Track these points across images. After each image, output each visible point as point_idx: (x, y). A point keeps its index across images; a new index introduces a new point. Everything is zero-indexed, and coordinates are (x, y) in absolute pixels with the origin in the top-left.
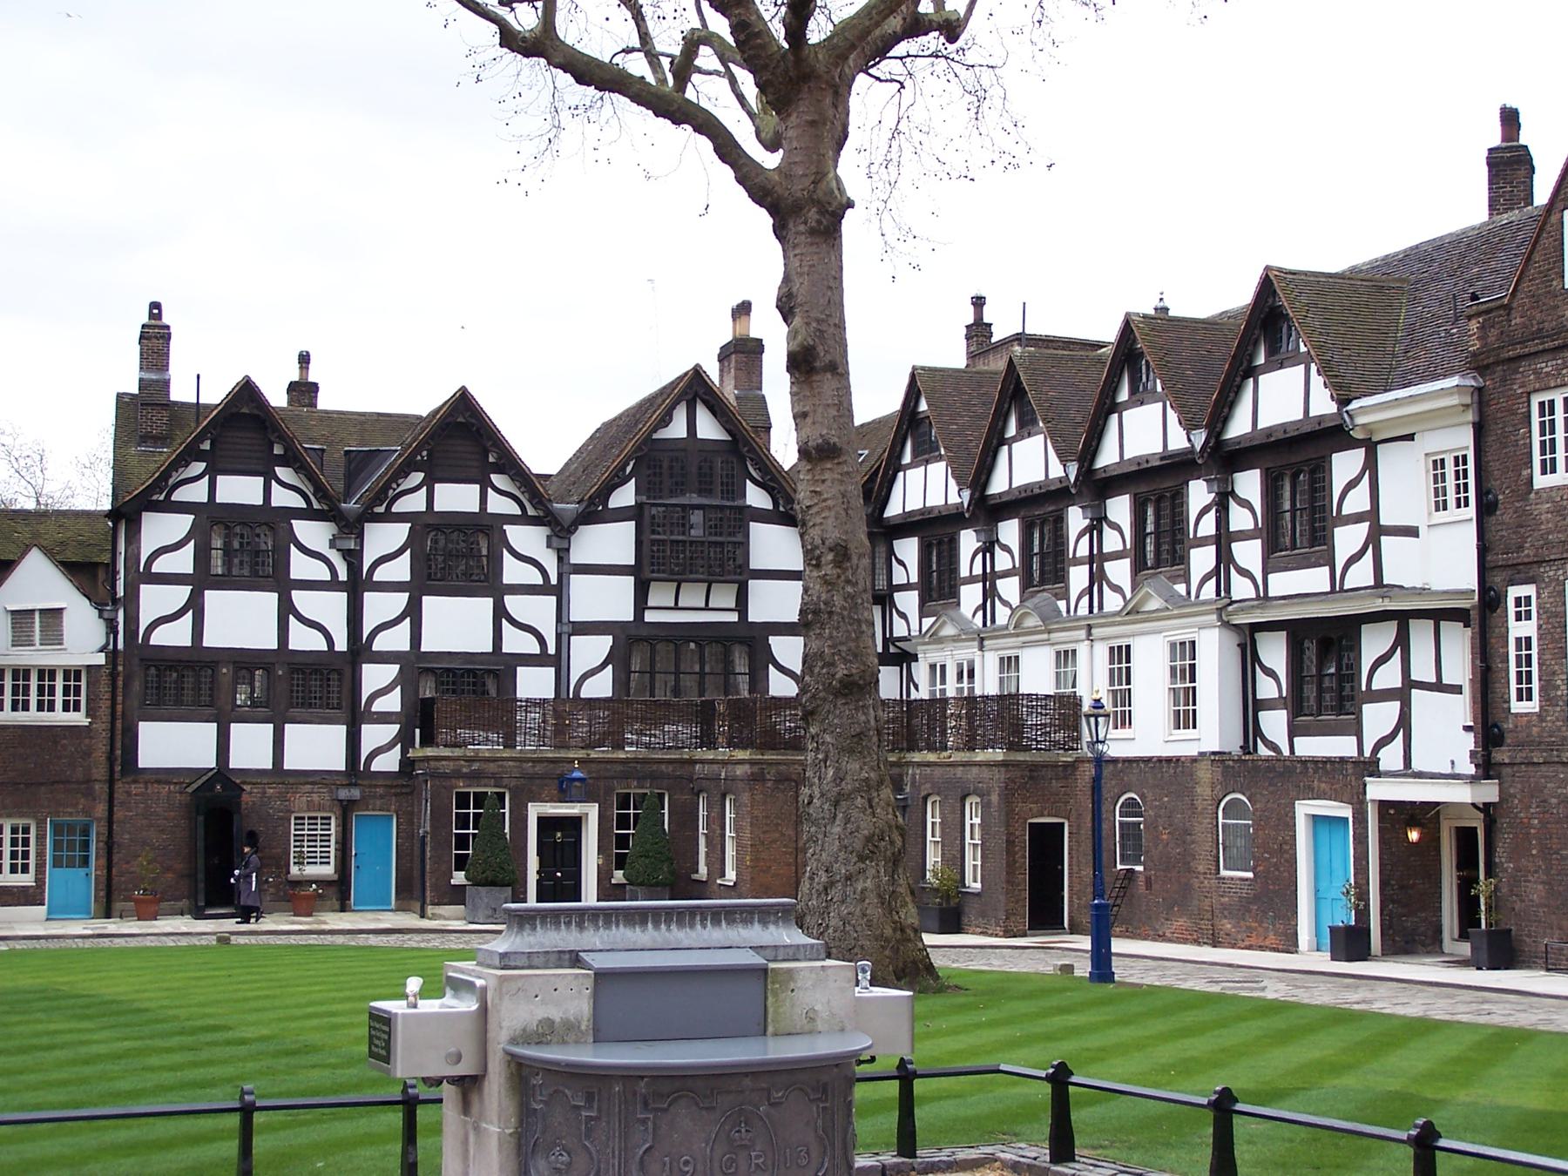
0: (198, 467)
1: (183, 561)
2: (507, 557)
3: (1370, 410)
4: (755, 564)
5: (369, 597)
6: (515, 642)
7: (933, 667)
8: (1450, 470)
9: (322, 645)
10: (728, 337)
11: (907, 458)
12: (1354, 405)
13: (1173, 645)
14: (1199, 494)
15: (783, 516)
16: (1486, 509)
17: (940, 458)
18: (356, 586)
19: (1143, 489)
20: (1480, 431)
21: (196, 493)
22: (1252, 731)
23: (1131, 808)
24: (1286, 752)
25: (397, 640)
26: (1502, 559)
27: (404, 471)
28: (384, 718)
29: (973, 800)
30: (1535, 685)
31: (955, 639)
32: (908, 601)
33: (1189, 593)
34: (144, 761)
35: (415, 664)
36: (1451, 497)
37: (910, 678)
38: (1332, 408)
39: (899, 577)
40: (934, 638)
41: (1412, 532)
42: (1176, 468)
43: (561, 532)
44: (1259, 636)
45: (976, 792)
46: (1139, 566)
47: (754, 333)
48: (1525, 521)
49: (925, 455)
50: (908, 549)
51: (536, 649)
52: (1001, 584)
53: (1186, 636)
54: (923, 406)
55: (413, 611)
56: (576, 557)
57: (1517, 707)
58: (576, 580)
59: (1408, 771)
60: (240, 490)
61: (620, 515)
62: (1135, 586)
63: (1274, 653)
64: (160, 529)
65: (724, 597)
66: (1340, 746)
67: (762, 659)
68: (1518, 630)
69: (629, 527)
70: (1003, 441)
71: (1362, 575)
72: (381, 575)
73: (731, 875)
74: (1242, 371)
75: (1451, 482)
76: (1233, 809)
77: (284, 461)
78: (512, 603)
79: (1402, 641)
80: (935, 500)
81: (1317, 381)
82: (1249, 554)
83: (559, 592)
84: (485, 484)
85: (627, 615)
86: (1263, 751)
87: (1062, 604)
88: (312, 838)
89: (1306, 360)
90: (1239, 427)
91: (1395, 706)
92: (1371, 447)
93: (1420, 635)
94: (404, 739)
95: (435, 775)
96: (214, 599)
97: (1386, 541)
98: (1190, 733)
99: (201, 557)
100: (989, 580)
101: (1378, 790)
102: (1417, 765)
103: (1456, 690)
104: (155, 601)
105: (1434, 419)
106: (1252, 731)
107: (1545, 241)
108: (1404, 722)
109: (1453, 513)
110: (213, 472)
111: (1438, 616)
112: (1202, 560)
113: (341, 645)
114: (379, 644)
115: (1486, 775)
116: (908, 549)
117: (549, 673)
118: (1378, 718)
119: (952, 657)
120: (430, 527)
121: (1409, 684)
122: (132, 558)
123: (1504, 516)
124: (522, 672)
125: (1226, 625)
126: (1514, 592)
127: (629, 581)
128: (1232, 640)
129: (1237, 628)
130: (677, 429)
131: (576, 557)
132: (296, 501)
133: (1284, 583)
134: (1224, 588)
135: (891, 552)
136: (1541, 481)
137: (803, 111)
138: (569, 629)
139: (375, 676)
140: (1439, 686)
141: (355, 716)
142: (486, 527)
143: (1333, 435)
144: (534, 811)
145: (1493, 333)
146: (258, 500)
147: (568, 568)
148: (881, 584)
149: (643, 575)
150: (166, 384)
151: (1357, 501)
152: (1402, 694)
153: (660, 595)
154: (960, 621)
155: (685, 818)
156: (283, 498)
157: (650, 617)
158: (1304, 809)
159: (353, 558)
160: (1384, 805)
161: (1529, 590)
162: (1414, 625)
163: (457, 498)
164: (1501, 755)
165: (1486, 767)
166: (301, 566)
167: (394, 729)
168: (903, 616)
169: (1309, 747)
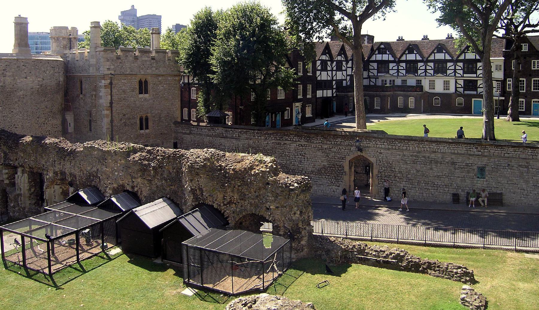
7: (382, 81)
16: (505, 70)
18: (332, 70)
22: (456, 90)
24: (462, 93)
30: (511, 88)
32: (375, 72)
33: (447, 75)
37: (370, 81)
50: (375, 65)
57: (508, 90)
63: (461, 82)
66: (475, 93)
68: (508, 83)
83: (346, 70)
87: (416, 74)
126: (508, 79)
133: (465, 75)
134: (455, 75)
141: (332, 89)
154: (390, 74)
161: (511, 79)
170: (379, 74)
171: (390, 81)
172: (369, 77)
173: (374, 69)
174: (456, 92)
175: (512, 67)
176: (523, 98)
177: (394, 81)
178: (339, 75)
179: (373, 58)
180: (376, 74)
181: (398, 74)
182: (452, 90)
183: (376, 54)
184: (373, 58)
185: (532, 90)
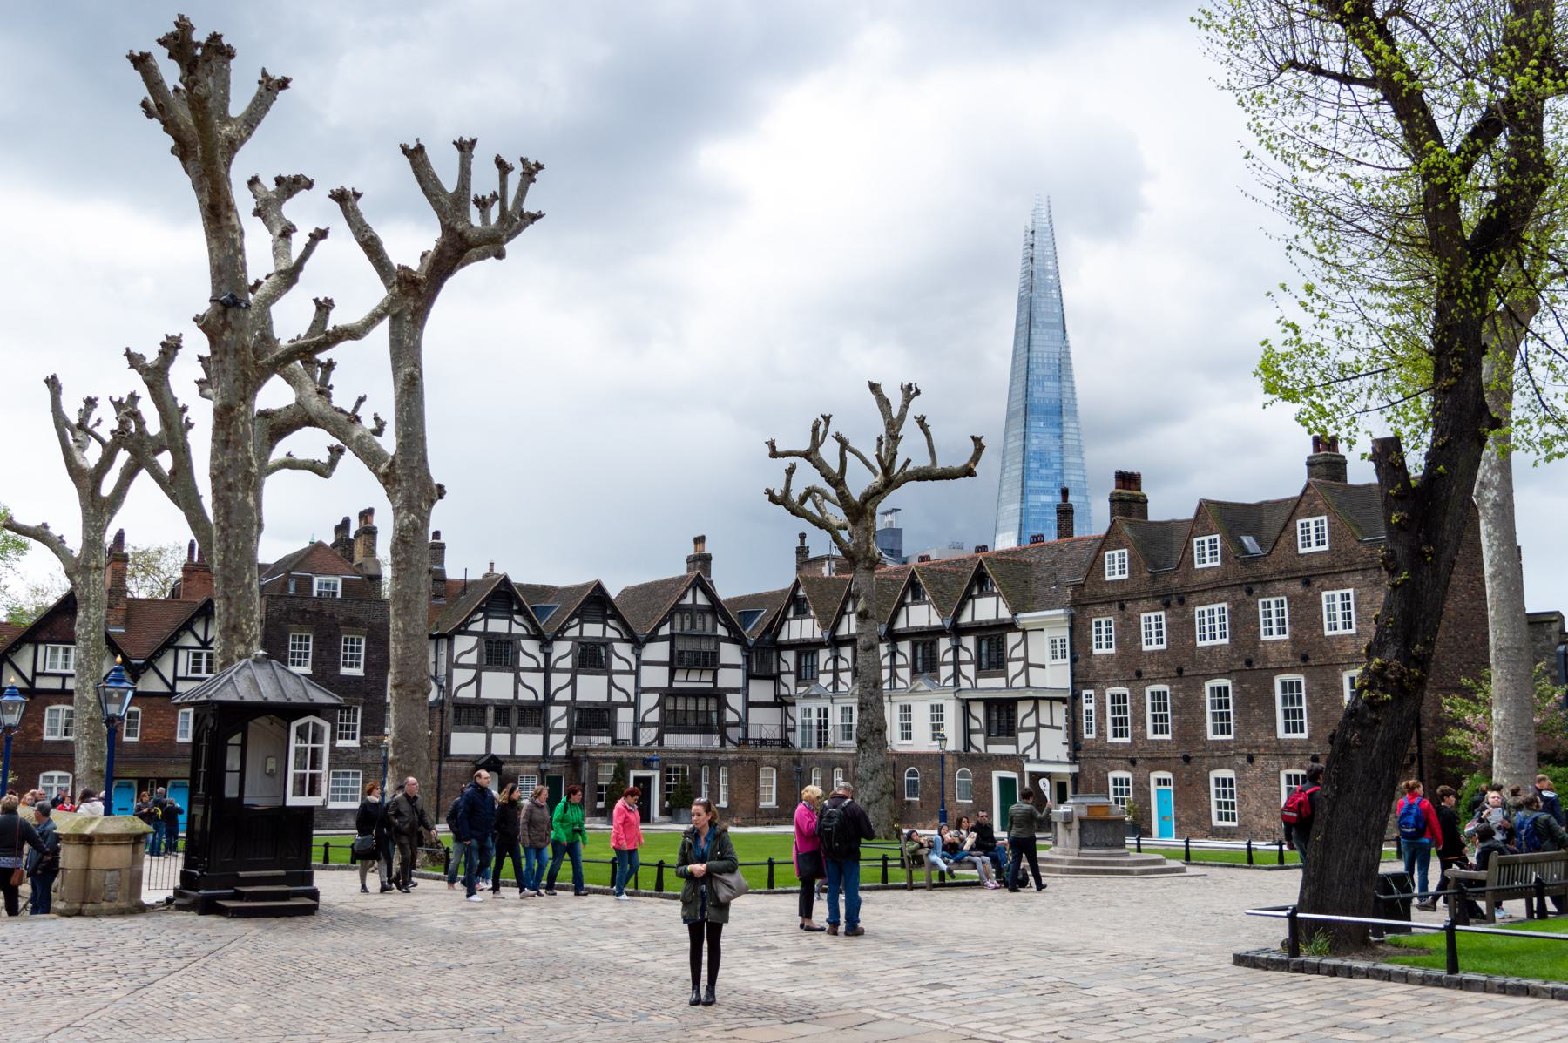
0: (481, 615)
1: (472, 658)
2: (614, 657)
3: (1025, 618)
4: (723, 661)
5: (554, 676)
6: (618, 697)
8: (1058, 644)
9: (532, 697)
10: (692, 553)
11: (791, 615)
12: (1020, 616)
13: (932, 706)
14: (944, 644)
15: (736, 638)
16: (1074, 660)
17: (810, 617)
18: (547, 670)
19: (916, 639)
20: (1072, 630)
21: (478, 627)
22: (968, 742)
23: (912, 774)
25: (565, 695)
26: (1080, 680)
27: (571, 618)
28: (559, 731)
29: (838, 770)
30: (1094, 728)
31: (818, 696)
32: (790, 680)
34: (453, 751)
35: (573, 706)
36: (1059, 654)
37: (787, 713)
38: (1010, 616)
39: (784, 667)
40: (807, 696)
41: (1043, 667)
42: (938, 632)
43: (638, 644)
44: (971, 704)
45: (841, 766)
46: (914, 671)
47: (707, 551)
48: (1089, 666)
49: (801, 613)
50: (790, 657)
51: (626, 700)
52: (841, 675)
53: (939, 702)
54: (801, 593)
55: (573, 682)
56: (644, 658)
58: (644, 668)
59: (1040, 761)
60: (498, 625)
61: (663, 639)
62: (913, 679)
63: (978, 711)
64: (463, 643)
65: (707, 677)
66: (1008, 749)
67: (722, 704)
68: (1086, 707)
69: (666, 645)
70: (845, 613)
71: (1020, 682)
72: (559, 665)
73: (723, 803)
74: (968, 596)
75: (1059, 649)
76: (963, 775)
77: (519, 612)
78: (616, 678)
79: (1036, 708)
80: (807, 635)
81: (1002, 605)
82: (968, 670)
83: (636, 673)
84: (605, 624)
85: (666, 684)
86: (973, 751)
88: (527, 787)
89: (998, 595)
90: (966, 619)
91: (1032, 734)
92: (1025, 632)
93: (1044, 708)
94: (569, 741)
95: (588, 757)
96: (484, 674)
97: (1031, 670)
98: (908, 742)
99: (480, 656)
100: (836, 672)
101: (1029, 768)
102: (1042, 758)
103: (1060, 728)
104: (460, 676)
105: (1054, 624)
106: (968, 742)
107: (1098, 562)
108: (1037, 741)
109: (1059, 661)
110: (486, 617)
111: (1051, 700)
112: (946, 671)
113: (541, 697)
114: (559, 697)
115: (1075, 763)
116: (790, 657)
117: (632, 710)
118: (1025, 739)
119: (814, 706)
120: (580, 643)
121: (1039, 725)
122: (450, 655)
123: (1081, 663)
124: (619, 709)
125: (957, 698)
126: (1085, 692)
127: (664, 672)
128: (960, 705)
129: (962, 700)
130: (688, 600)
131: (644, 658)
132: (522, 631)
133: (984, 683)
134: (957, 683)
135: (779, 656)
136: (1096, 651)
137: (862, 524)
138: (640, 690)
139: (556, 712)
140: (1052, 727)
142: (606, 643)
143: (1011, 626)
144: (633, 774)
145: (1077, 594)
146: (506, 631)
147: (640, 663)
148: (775, 670)
149: (673, 665)
150: (443, 572)
151: (1019, 653)
152: (1036, 729)
153: (680, 676)
155: (697, 778)
156: (517, 630)
157: (675, 685)
158: (996, 775)
159: (548, 656)
160: (1031, 773)
161: (1091, 692)
162: (1041, 702)
163: (593, 630)
164: (1080, 755)
165: (1074, 759)
166: (525, 661)
167: (563, 737)
168: (786, 686)
169: (994, 749)
170: (801, 690)
171: (819, 710)
172: (782, 703)
173: (789, 672)
174: (966, 749)
175: (1091, 644)
176: (1126, 769)
177: (826, 710)
178: (592, 688)
179: (783, 637)
180: (793, 693)
181: (836, 689)
182: (953, 743)
183: (789, 620)
184: (783, 637)
185: (1151, 735)
